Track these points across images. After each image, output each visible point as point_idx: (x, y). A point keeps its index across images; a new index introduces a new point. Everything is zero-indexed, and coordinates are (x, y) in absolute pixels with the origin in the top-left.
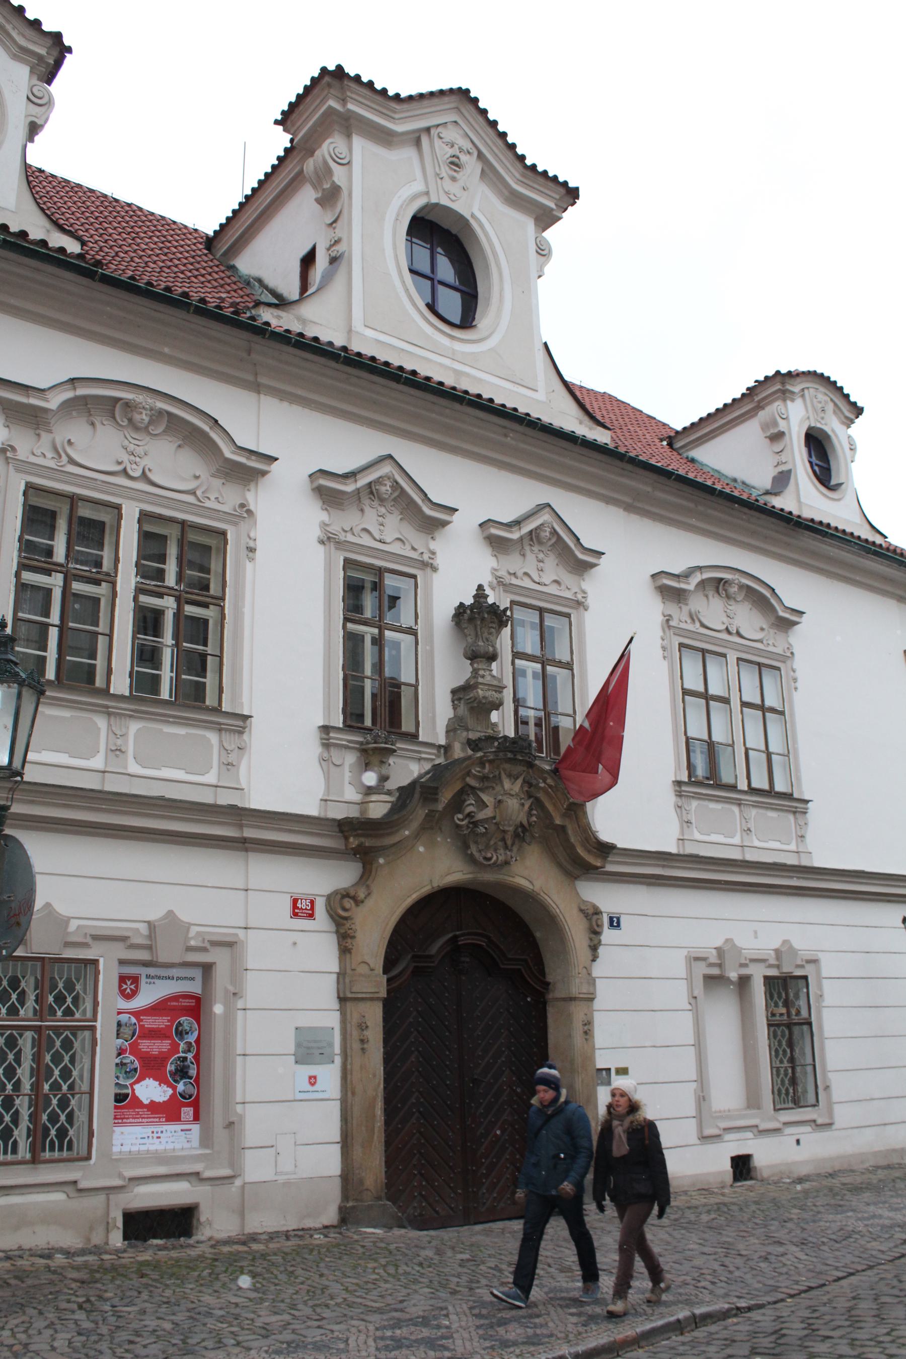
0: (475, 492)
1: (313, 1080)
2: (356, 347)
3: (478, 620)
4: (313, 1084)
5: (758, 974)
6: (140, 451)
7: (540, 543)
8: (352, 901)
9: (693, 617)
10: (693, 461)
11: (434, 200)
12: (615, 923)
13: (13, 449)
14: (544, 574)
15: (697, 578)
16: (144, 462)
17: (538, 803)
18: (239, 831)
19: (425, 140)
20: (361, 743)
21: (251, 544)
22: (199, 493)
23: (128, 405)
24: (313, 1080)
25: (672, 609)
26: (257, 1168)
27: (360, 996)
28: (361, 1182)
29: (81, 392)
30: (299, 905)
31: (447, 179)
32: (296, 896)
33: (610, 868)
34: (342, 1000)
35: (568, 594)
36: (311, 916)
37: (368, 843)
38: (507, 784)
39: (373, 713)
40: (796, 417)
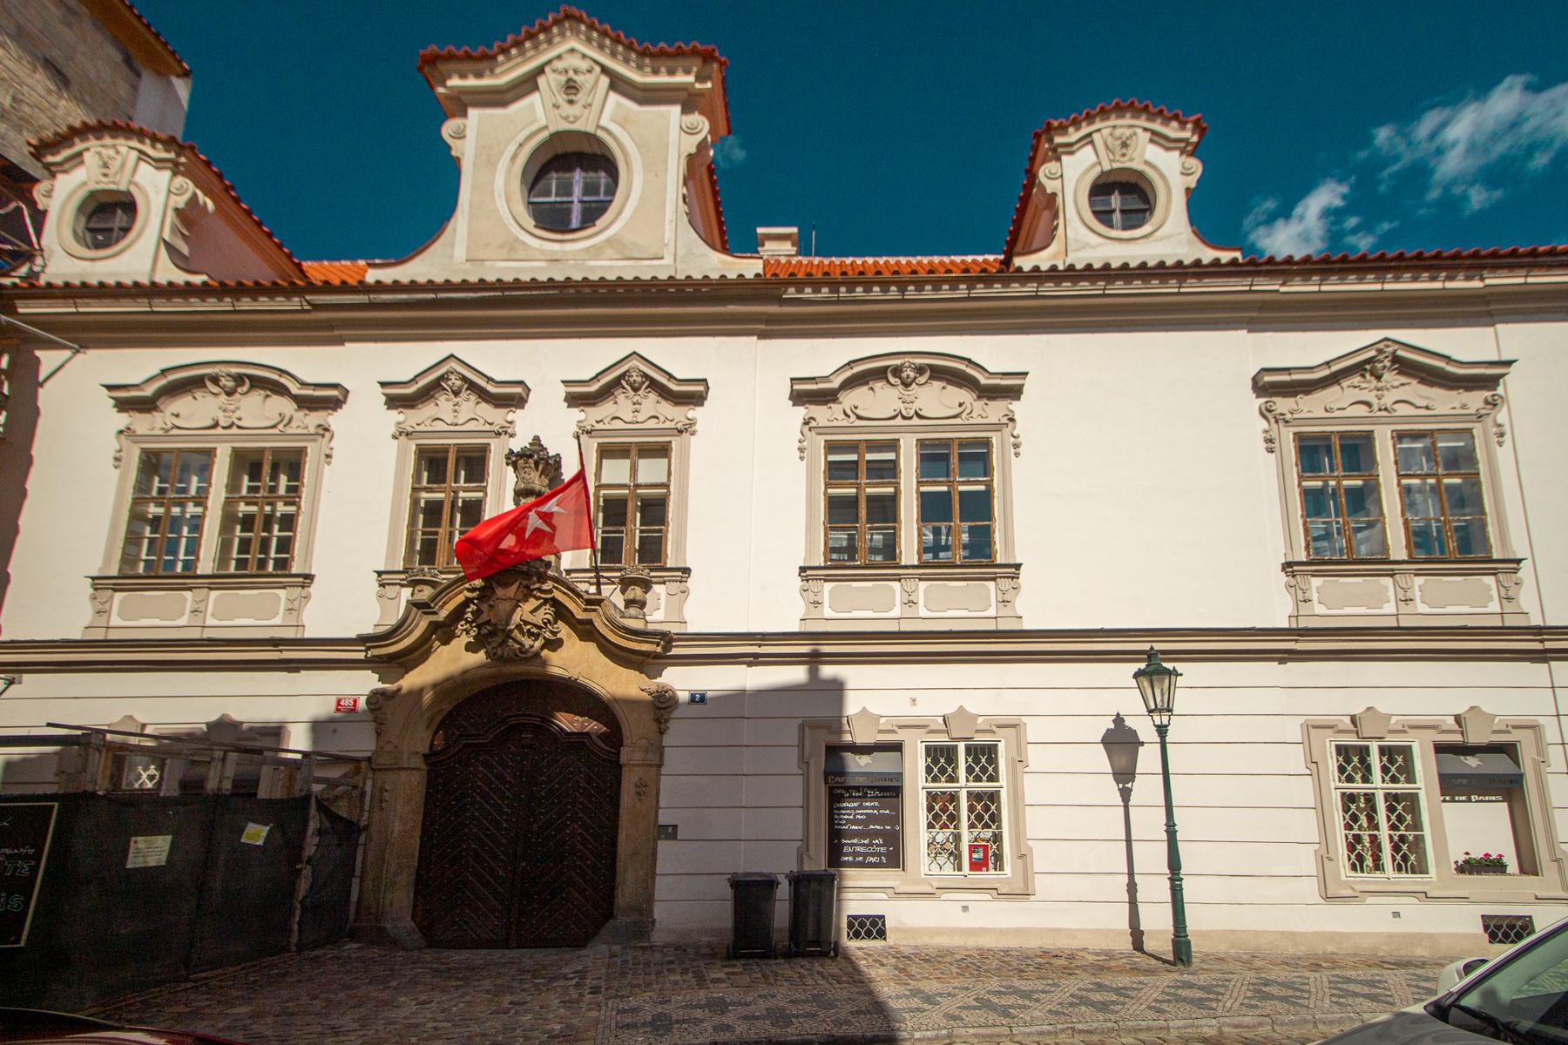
16: (238, 414)
23: (215, 380)
35: (668, 425)
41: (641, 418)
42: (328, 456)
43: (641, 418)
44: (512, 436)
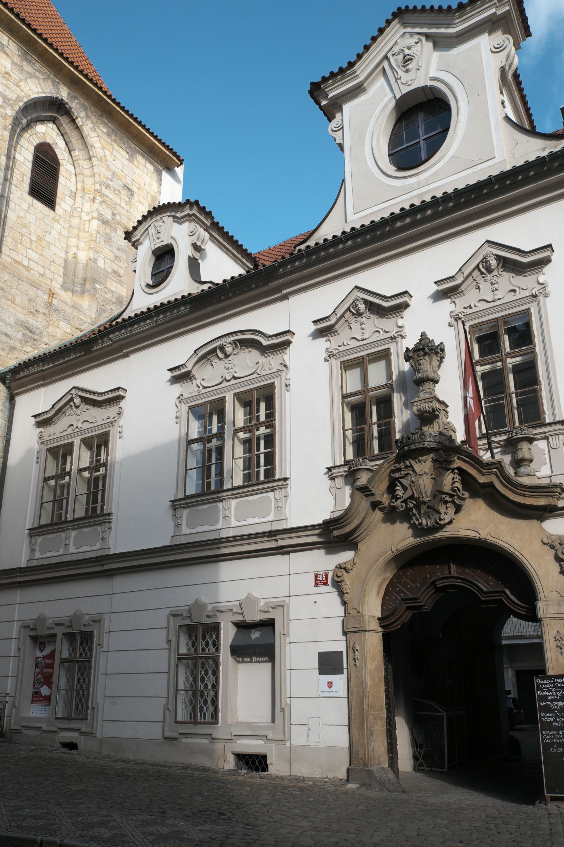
1: (330, 685)
4: (330, 687)
8: (343, 571)
18: (277, 543)
24: (330, 685)
26: (298, 737)
27: (352, 630)
28: (357, 753)
30: (318, 578)
32: (317, 573)
34: (345, 633)
36: (326, 584)
41: (499, 295)
42: (287, 386)
43: (499, 295)
44: (403, 337)
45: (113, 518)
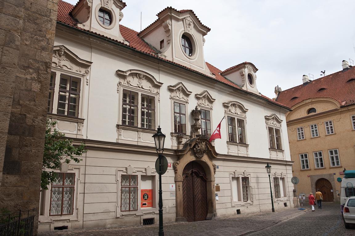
0: (194, 89)
2: (174, 61)
3: (195, 114)
5: (241, 176)
6: (141, 82)
7: (205, 98)
9: (230, 111)
10: (225, 78)
11: (186, 32)
12: (218, 167)
13: (121, 83)
14: (205, 104)
15: (230, 104)
17: (207, 147)
19: (184, 20)
20: (177, 136)
21: (159, 99)
22: (151, 90)
23: (139, 74)
25: (226, 109)
29: (132, 72)
31: (188, 28)
33: (218, 157)
34: (175, 182)
37: (180, 154)
38: (203, 143)
39: (179, 130)
40: (246, 71)
45: (85, 121)
